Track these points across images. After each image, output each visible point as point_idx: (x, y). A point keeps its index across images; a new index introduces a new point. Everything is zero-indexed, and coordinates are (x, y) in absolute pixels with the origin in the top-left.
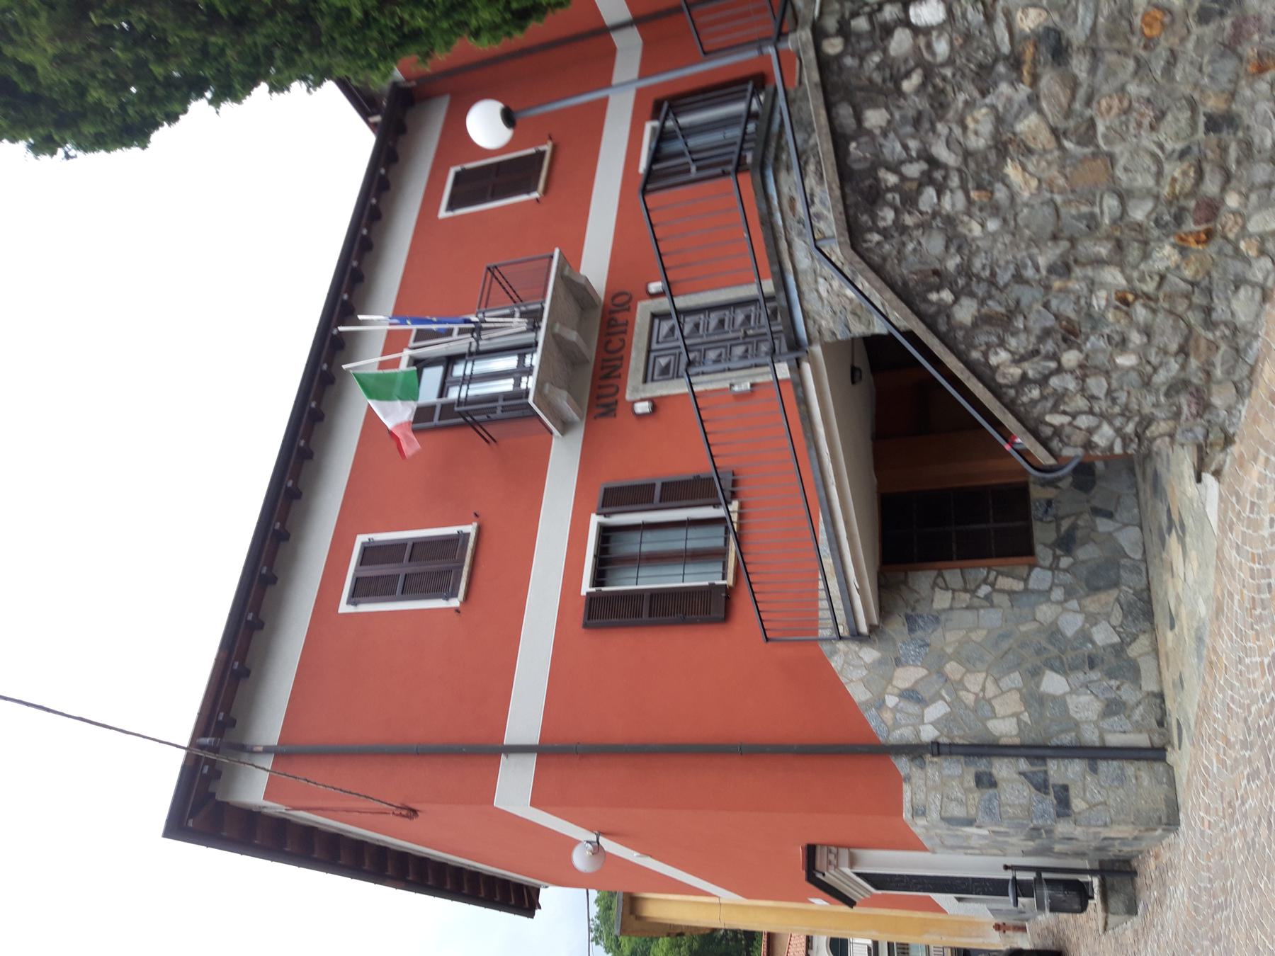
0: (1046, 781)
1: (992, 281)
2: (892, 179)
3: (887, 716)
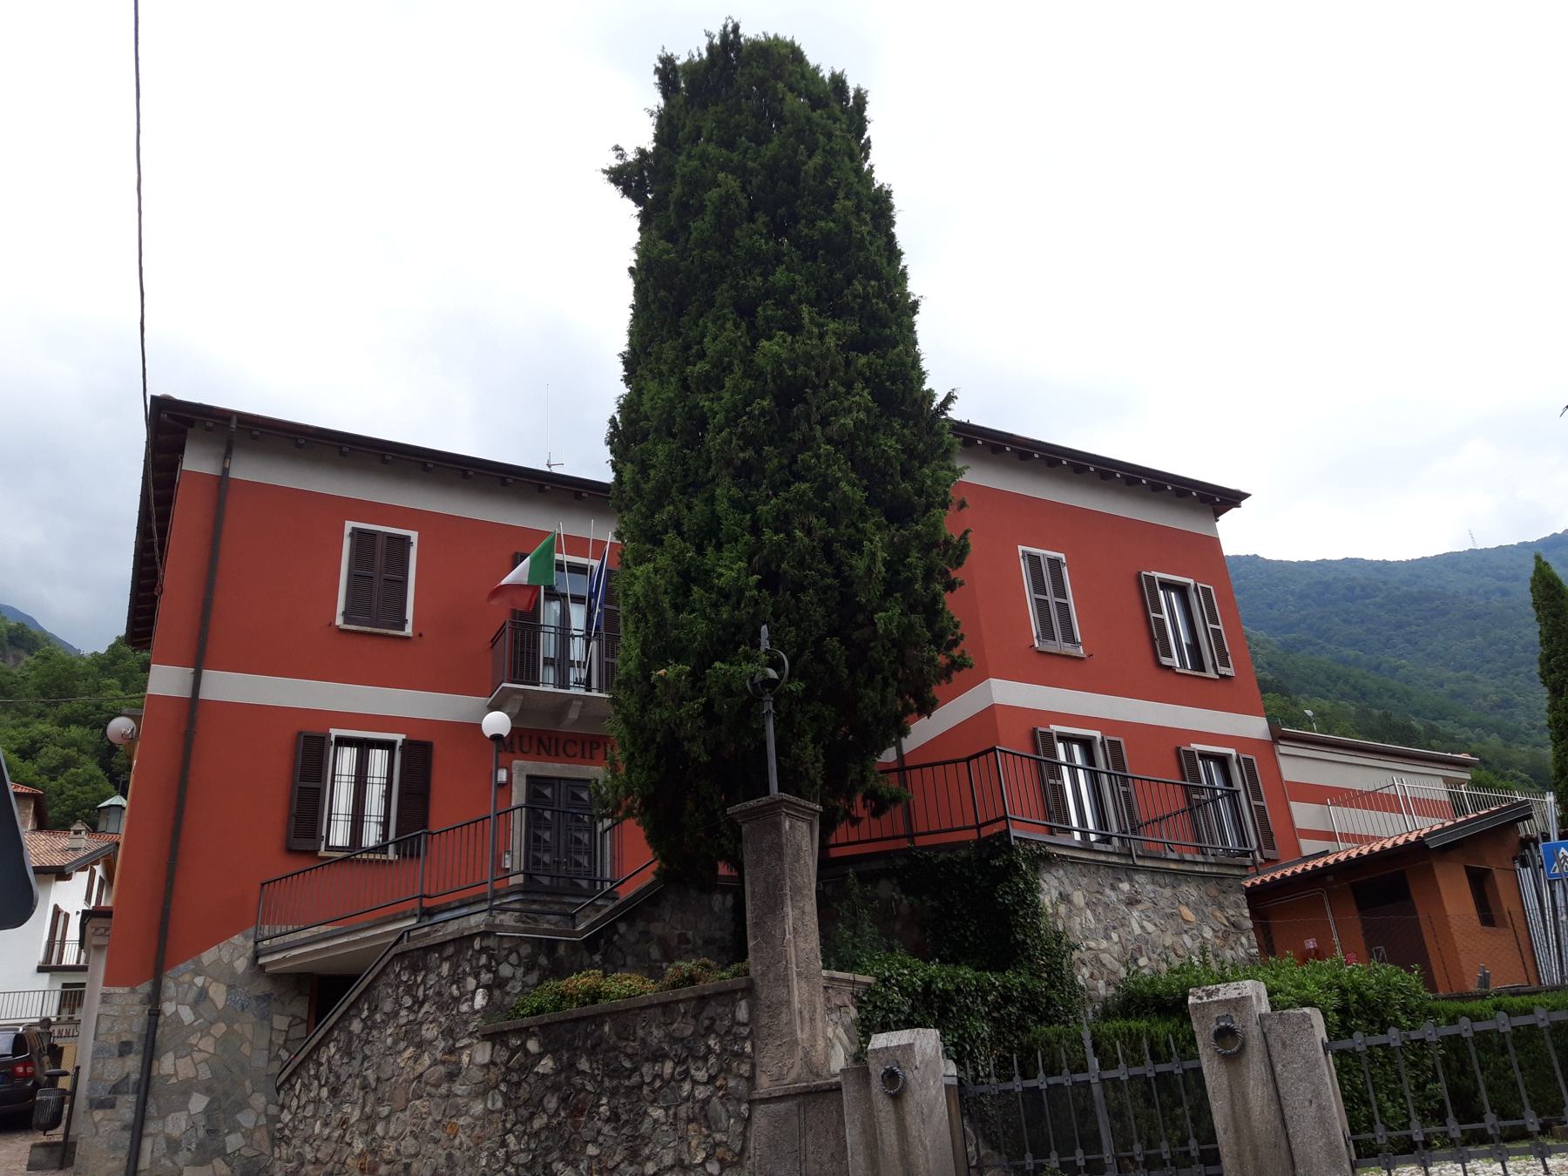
0: (120, 1093)
1: (367, 1042)
2: (419, 979)
3: (187, 978)
